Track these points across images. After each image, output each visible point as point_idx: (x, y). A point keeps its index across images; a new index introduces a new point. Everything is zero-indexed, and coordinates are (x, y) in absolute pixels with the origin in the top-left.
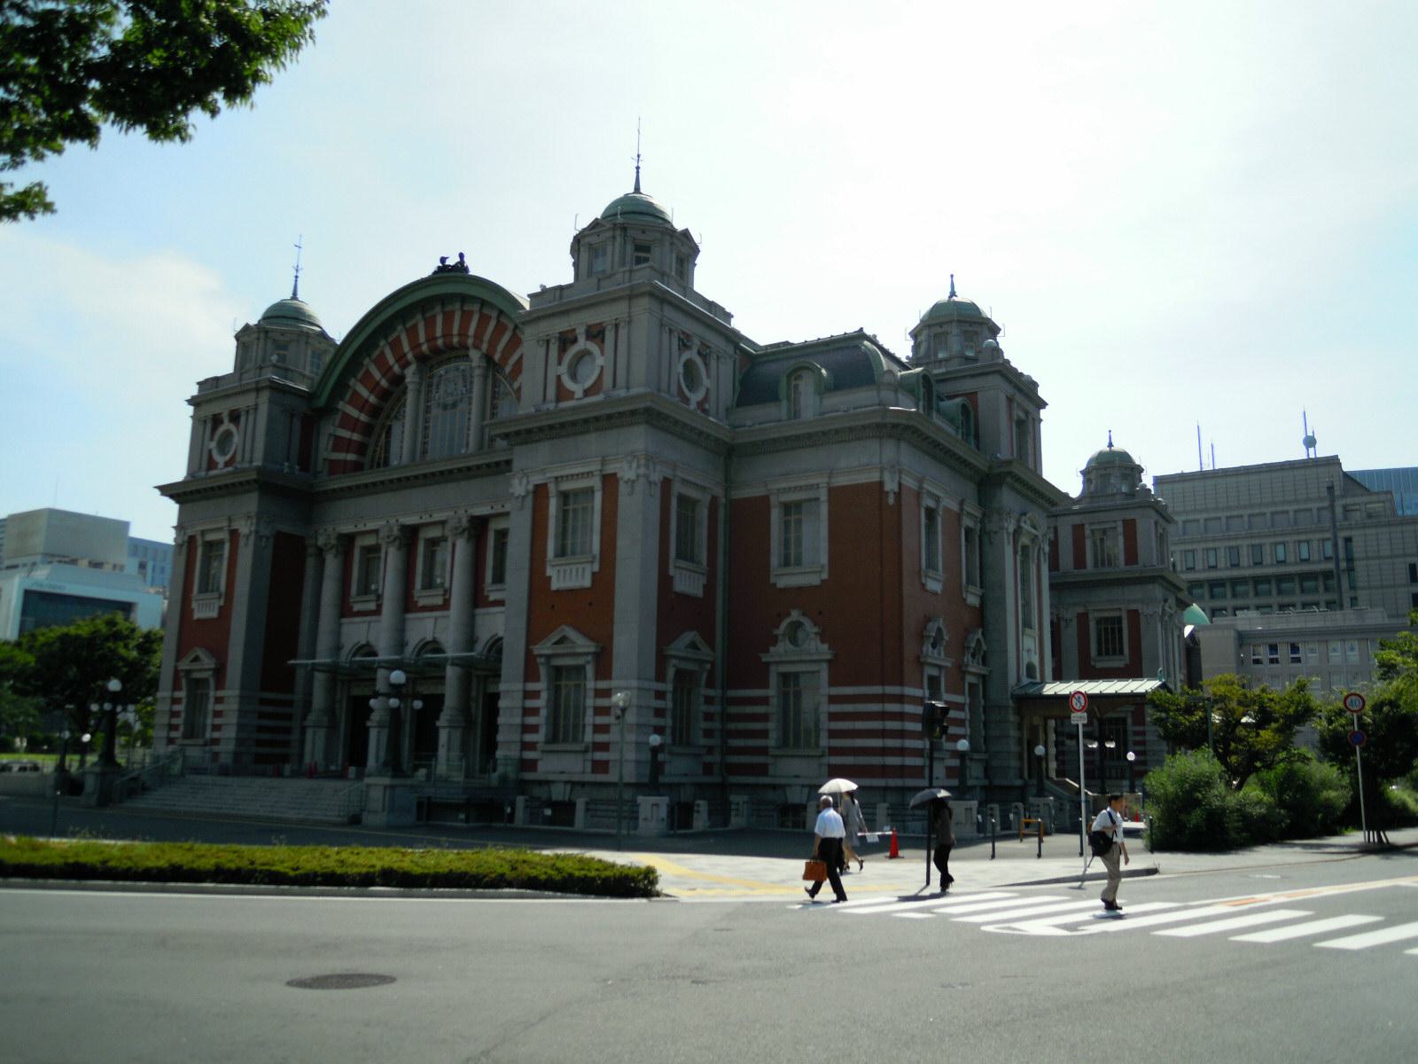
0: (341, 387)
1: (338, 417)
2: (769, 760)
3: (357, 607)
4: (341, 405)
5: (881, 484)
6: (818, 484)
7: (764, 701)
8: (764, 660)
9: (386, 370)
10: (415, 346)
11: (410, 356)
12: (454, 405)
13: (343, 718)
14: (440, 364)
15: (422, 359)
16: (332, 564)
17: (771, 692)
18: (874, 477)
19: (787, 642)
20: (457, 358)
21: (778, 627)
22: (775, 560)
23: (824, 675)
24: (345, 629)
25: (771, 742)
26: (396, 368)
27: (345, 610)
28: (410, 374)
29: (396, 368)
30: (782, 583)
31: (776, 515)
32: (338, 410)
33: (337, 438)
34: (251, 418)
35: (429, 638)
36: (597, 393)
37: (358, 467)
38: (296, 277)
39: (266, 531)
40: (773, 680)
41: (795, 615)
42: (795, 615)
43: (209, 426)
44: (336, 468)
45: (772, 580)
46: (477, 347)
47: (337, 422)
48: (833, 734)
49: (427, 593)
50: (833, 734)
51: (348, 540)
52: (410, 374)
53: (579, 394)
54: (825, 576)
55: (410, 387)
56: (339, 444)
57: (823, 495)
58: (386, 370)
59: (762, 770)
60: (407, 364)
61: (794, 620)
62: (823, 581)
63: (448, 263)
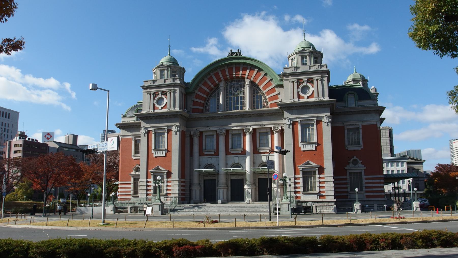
0: (197, 85)
1: (195, 94)
2: (348, 194)
3: (206, 153)
4: (196, 92)
5: (377, 125)
6: (359, 124)
7: (346, 179)
8: (346, 169)
9: (213, 82)
10: (225, 76)
11: (222, 79)
13: (203, 186)
14: (231, 81)
15: (226, 80)
16: (196, 140)
17: (348, 177)
18: (375, 123)
19: (352, 164)
20: (241, 81)
21: (350, 160)
22: (346, 143)
23: (363, 173)
24: (201, 160)
25: (349, 190)
26: (217, 82)
27: (201, 154)
28: (222, 85)
29: (217, 82)
30: (349, 149)
31: (346, 131)
32: (195, 93)
33: (194, 101)
34: (172, 94)
35: (209, 163)
36: (313, 97)
37: (202, 111)
38: (169, 49)
39: (181, 131)
40: (348, 174)
41: (355, 158)
42: (355, 158)
43: (152, 96)
44: (194, 111)
45: (346, 148)
46: (248, 78)
47: (194, 96)
48: (366, 187)
49: (233, 149)
50: (366, 187)
51: (201, 133)
53: (306, 97)
54: (362, 148)
55: (221, 88)
56: (195, 103)
57: (361, 127)
58: (213, 82)
59: (346, 197)
60: (221, 81)
61: (355, 159)
62: (361, 149)
63: (233, 51)
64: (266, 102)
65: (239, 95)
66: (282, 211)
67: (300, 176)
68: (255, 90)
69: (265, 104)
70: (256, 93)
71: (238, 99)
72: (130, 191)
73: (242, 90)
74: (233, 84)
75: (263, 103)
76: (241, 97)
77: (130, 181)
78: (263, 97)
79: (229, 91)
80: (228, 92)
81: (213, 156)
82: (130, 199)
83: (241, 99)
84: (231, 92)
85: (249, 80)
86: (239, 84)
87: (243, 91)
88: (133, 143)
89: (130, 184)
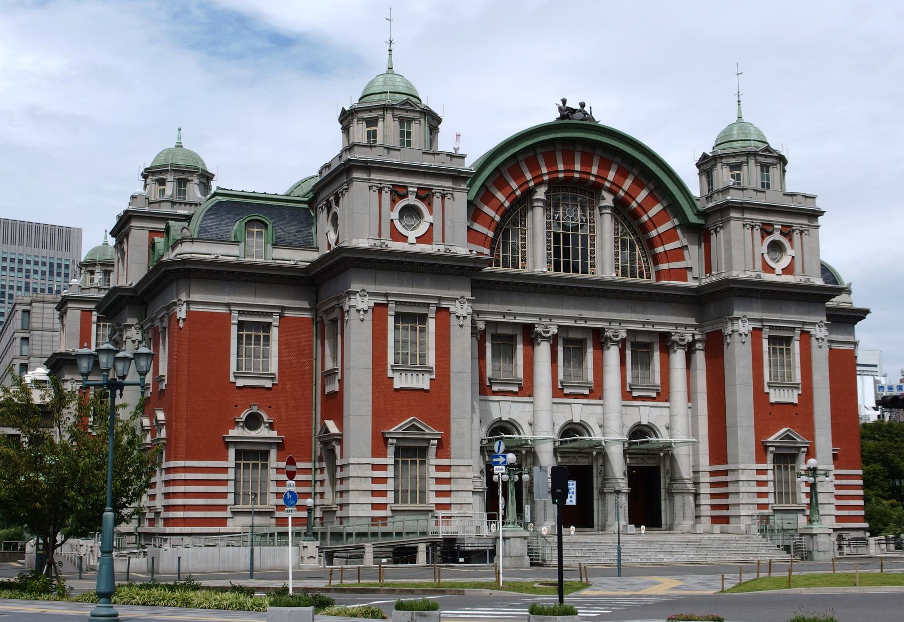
12: (575, 228)
28: (541, 193)
46: (610, 191)
52: (541, 193)
60: (541, 183)
64: (644, 261)
65: (578, 231)
66: (817, 552)
67: (769, 466)
69: (643, 266)
70: (621, 232)
71: (575, 243)
72: (224, 495)
73: (586, 220)
74: (564, 198)
76: (584, 238)
77: (225, 458)
78: (637, 248)
79: (554, 217)
80: (550, 218)
81: (516, 399)
82: (222, 522)
83: (584, 244)
85: (612, 197)
86: (579, 199)
87: (590, 222)
88: (234, 330)
89: (224, 470)
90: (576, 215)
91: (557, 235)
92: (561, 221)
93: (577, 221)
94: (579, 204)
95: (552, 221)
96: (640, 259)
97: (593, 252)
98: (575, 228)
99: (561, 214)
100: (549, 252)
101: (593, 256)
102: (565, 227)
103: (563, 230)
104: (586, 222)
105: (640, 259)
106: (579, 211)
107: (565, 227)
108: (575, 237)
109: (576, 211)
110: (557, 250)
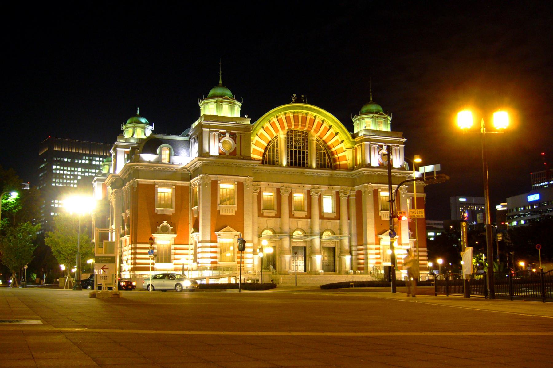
3: (265, 214)
65: (301, 149)
68: (318, 146)
75: (327, 162)
76: (304, 152)
78: (327, 155)
84: (293, 144)
87: (306, 145)
90: (300, 142)
91: (292, 151)
92: (294, 145)
93: (301, 145)
94: (301, 138)
95: (290, 145)
96: (328, 160)
97: (307, 158)
98: (300, 148)
99: (294, 142)
100: (288, 158)
101: (307, 159)
102: (295, 147)
103: (295, 148)
104: (304, 145)
105: (328, 160)
106: (301, 141)
107: (295, 147)
108: (300, 152)
109: (300, 140)
110: (292, 157)
